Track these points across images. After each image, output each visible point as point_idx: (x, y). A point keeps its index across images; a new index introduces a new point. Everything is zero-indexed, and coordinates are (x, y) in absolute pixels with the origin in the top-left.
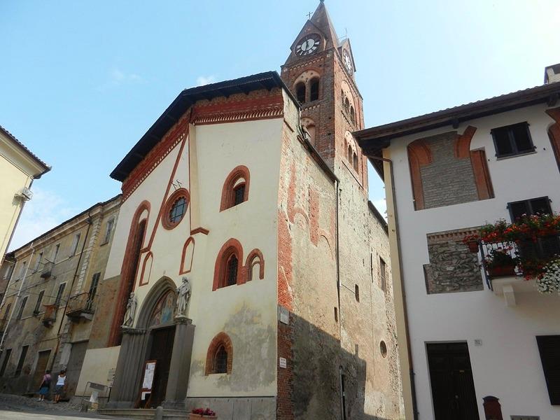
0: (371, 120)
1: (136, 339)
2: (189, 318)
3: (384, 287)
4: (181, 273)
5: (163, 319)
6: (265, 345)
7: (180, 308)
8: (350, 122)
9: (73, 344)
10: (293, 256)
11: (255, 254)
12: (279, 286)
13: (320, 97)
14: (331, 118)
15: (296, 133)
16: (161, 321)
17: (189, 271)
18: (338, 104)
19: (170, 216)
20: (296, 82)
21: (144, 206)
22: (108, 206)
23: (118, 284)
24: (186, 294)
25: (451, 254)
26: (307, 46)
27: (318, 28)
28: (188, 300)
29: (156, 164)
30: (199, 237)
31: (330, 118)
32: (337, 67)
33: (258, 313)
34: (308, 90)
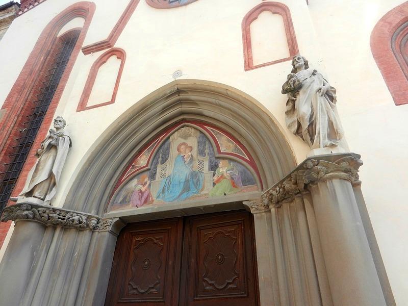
1: (61, 242)
4: (249, 65)
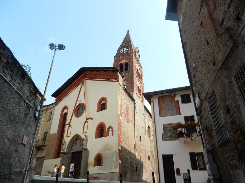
0: (147, 90)
2: (87, 148)
3: (149, 136)
4: (83, 133)
5: (76, 149)
6: (114, 156)
7: (84, 145)
8: (138, 78)
9: (37, 158)
10: (122, 128)
11: (110, 127)
12: (119, 138)
13: (128, 69)
14: (132, 78)
15: (122, 87)
16: (76, 149)
17: (86, 132)
18: (135, 72)
19: (77, 112)
20: (120, 63)
21: (66, 108)
22: (50, 107)
23: (57, 136)
24: (86, 140)
25: (169, 130)
26: (124, 50)
27: (127, 43)
28: (87, 142)
29: (70, 92)
30: (89, 121)
31: (132, 78)
32: (134, 59)
33: (112, 147)
34: (124, 66)
